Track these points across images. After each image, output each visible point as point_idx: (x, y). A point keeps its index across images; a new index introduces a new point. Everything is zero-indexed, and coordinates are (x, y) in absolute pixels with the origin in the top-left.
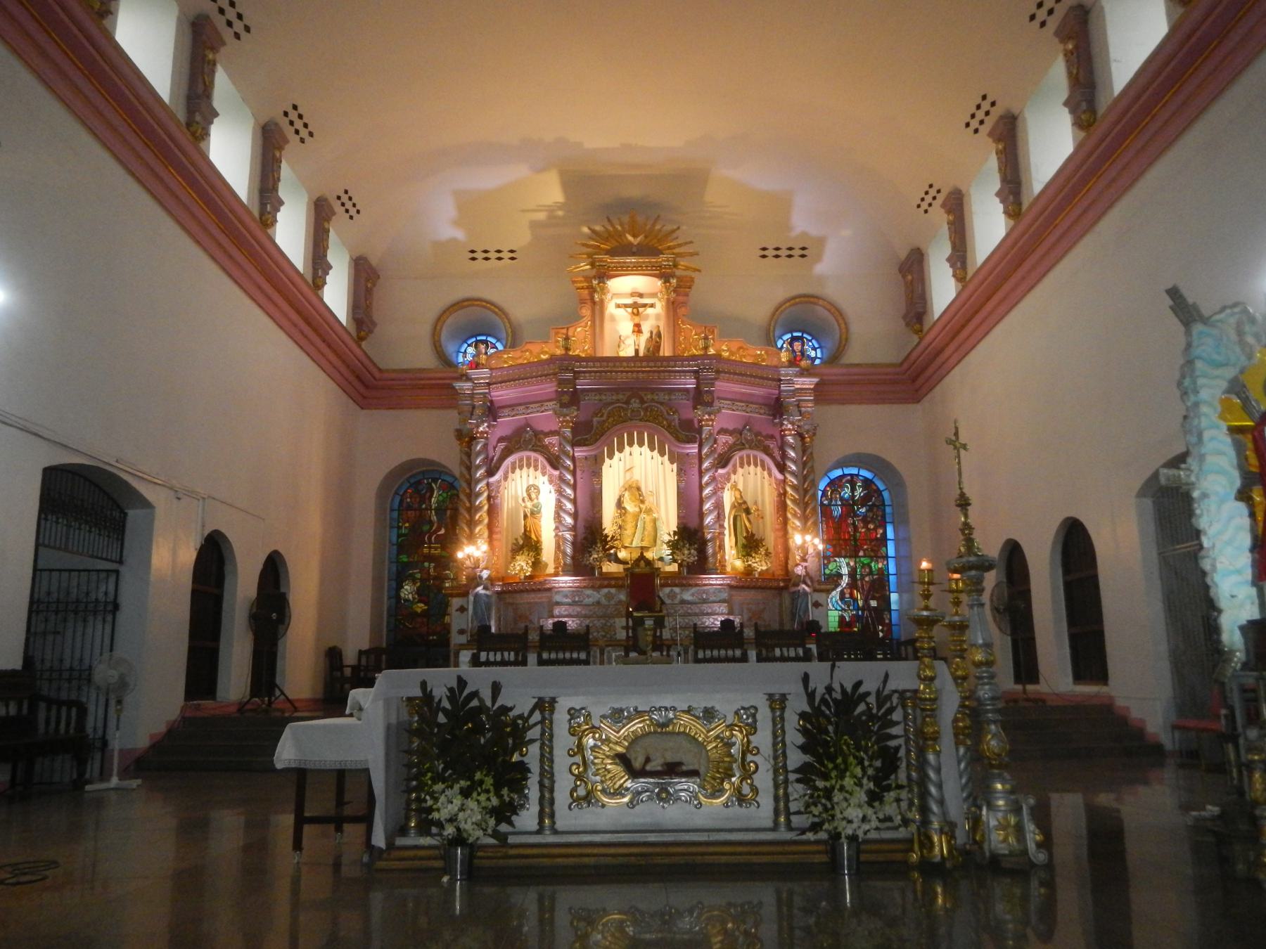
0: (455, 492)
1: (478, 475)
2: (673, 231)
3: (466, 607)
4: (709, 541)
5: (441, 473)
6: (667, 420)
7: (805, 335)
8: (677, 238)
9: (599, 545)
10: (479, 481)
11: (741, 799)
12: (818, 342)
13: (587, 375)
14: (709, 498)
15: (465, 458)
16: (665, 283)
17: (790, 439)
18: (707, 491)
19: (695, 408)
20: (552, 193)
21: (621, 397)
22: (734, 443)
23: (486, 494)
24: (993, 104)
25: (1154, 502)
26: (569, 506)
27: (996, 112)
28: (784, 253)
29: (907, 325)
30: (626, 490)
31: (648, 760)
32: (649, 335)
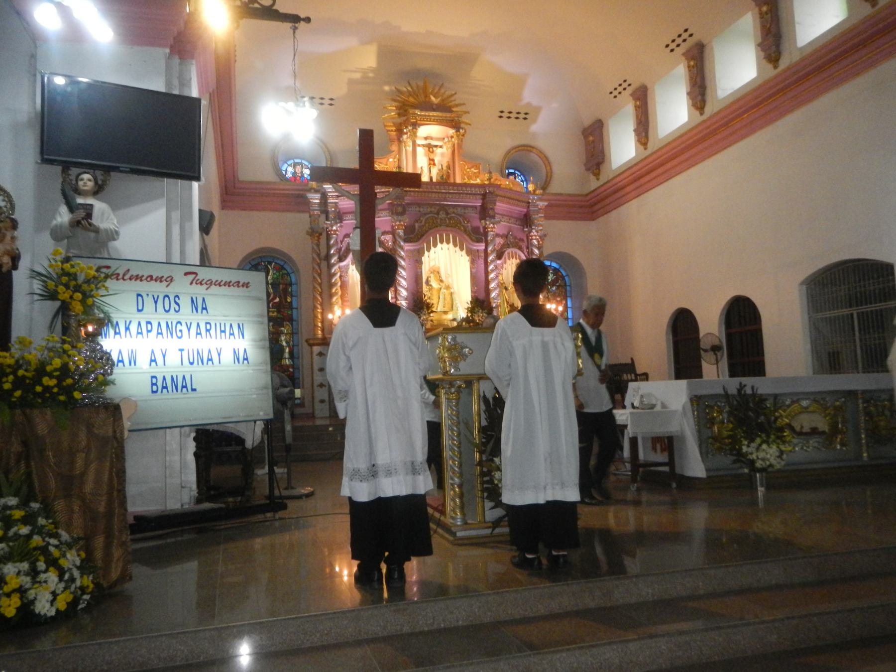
0: (285, 272)
1: (333, 261)
2: (452, 95)
3: (324, 352)
4: (495, 308)
5: (274, 258)
6: (463, 226)
7: (516, 172)
8: (455, 100)
9: (425, 310)
10: (334, 265)
11: (843, 444)
12: (524, 176)
13: (412, 193)
14: (493, 280)
15: (315, 247)
16: (457, 132)
17: (535, 242)
18: (492, 276)
19: (481, 219)
20: (369, 59)
21: (433, 209)
22: (504, 244)
23: (339, 274)
24: (691, 35)
25: (807, 289)
26: (404, 283)
27: (691, 42)
28: (513, 115)
29: (588, 169)
30: (431, 273)
31: (802, 427)
32: (440, 167)
